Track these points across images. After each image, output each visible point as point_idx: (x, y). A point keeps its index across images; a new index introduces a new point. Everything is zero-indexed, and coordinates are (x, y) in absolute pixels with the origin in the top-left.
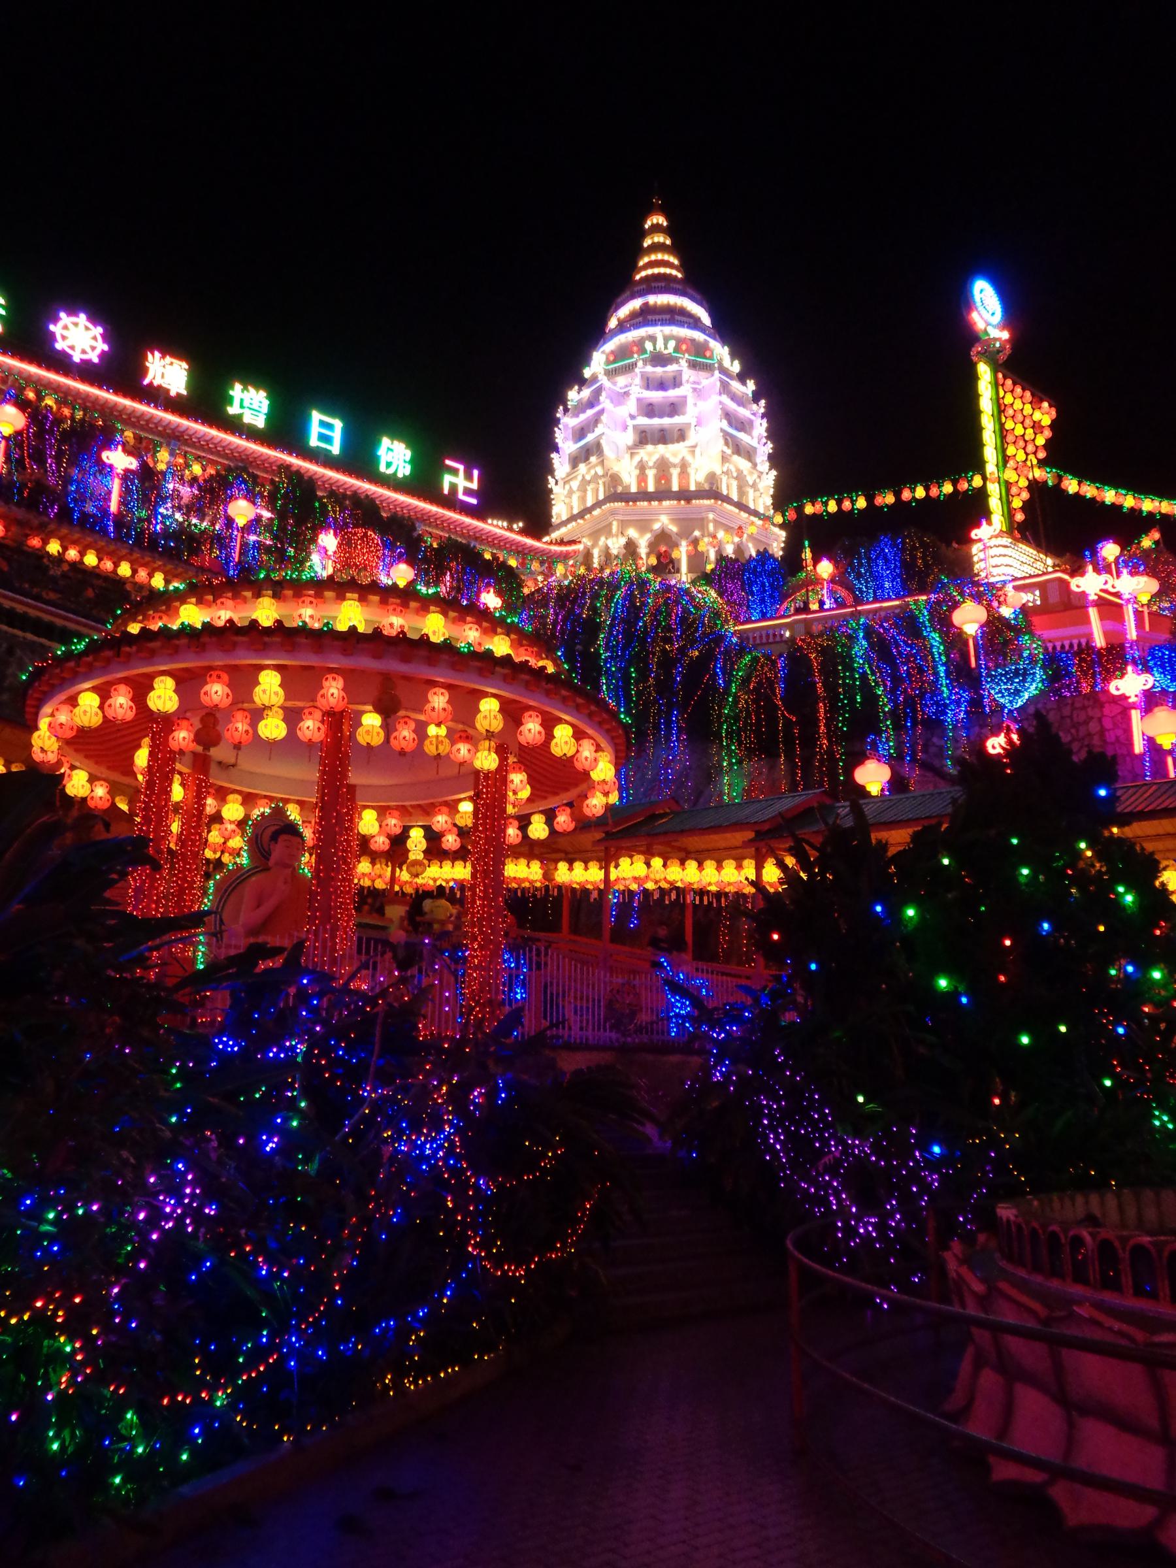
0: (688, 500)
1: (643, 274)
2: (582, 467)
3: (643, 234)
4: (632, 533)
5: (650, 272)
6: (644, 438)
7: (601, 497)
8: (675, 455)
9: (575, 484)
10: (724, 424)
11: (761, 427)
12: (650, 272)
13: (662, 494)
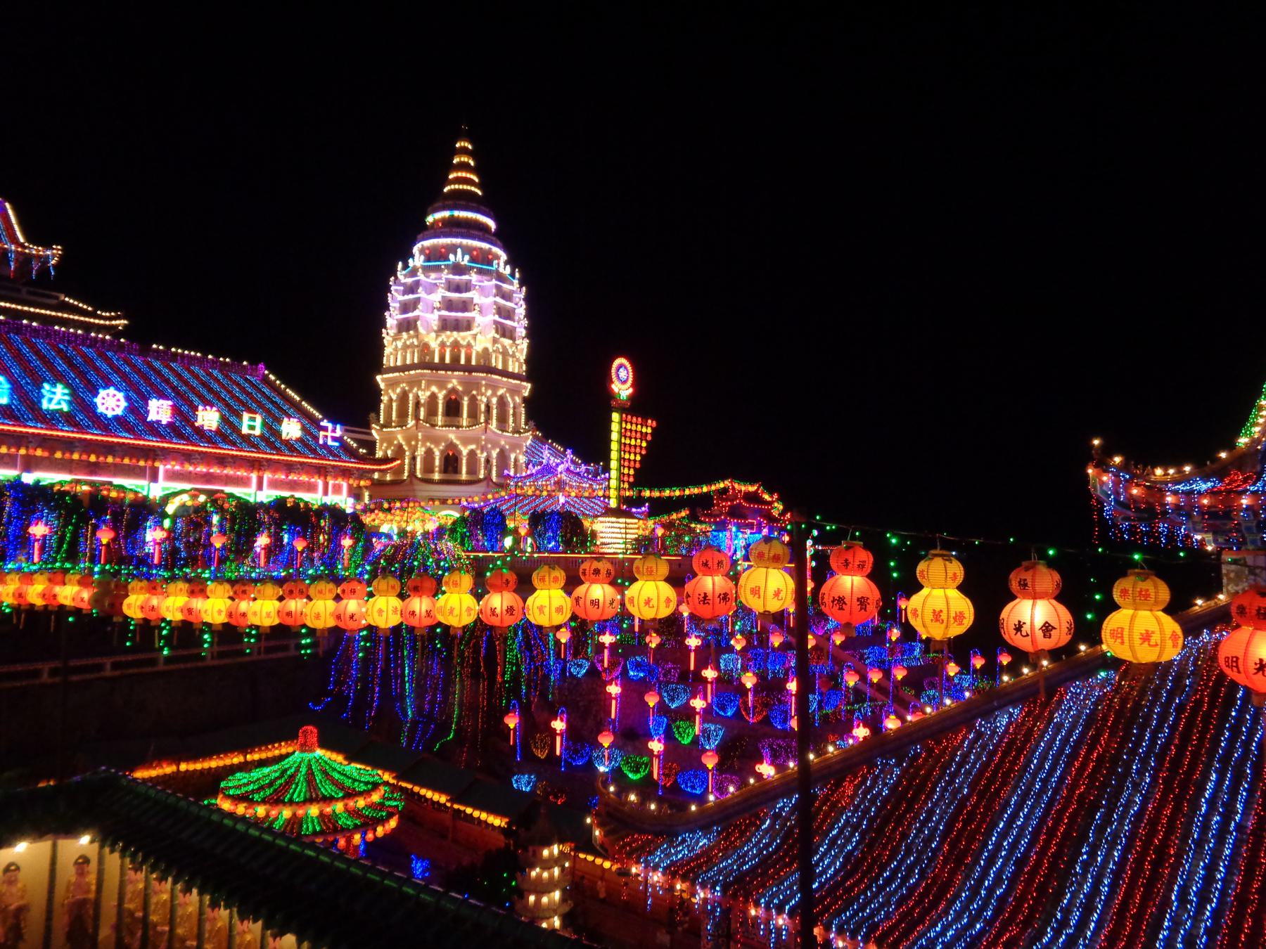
0: (470, 372)
2: (405, 335)
4: (434, 389)
6: (445, 325)
7: (416, 361)
8: (464, 338)
9: (400, 344)
10: (497, 318)
11: (521, 311)
13: (455, 366)
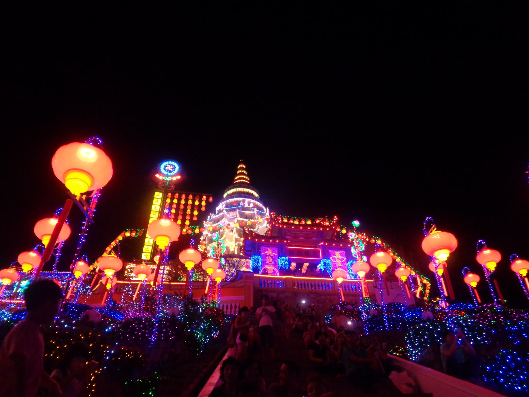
1: (237, 181)
3: (237, 170)
5: (239, 181)
12: (239, 181)
